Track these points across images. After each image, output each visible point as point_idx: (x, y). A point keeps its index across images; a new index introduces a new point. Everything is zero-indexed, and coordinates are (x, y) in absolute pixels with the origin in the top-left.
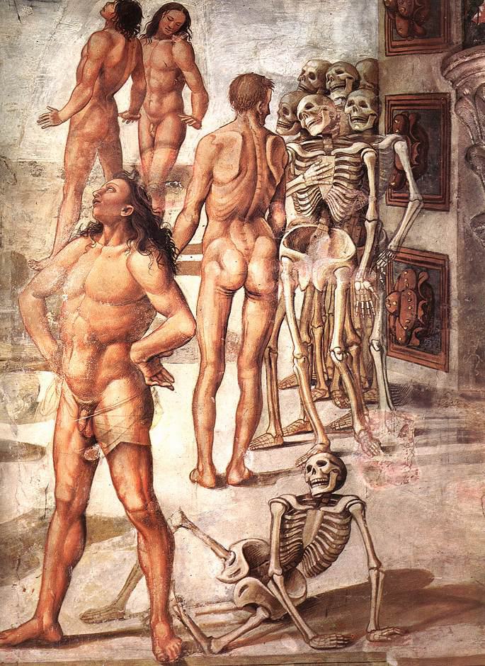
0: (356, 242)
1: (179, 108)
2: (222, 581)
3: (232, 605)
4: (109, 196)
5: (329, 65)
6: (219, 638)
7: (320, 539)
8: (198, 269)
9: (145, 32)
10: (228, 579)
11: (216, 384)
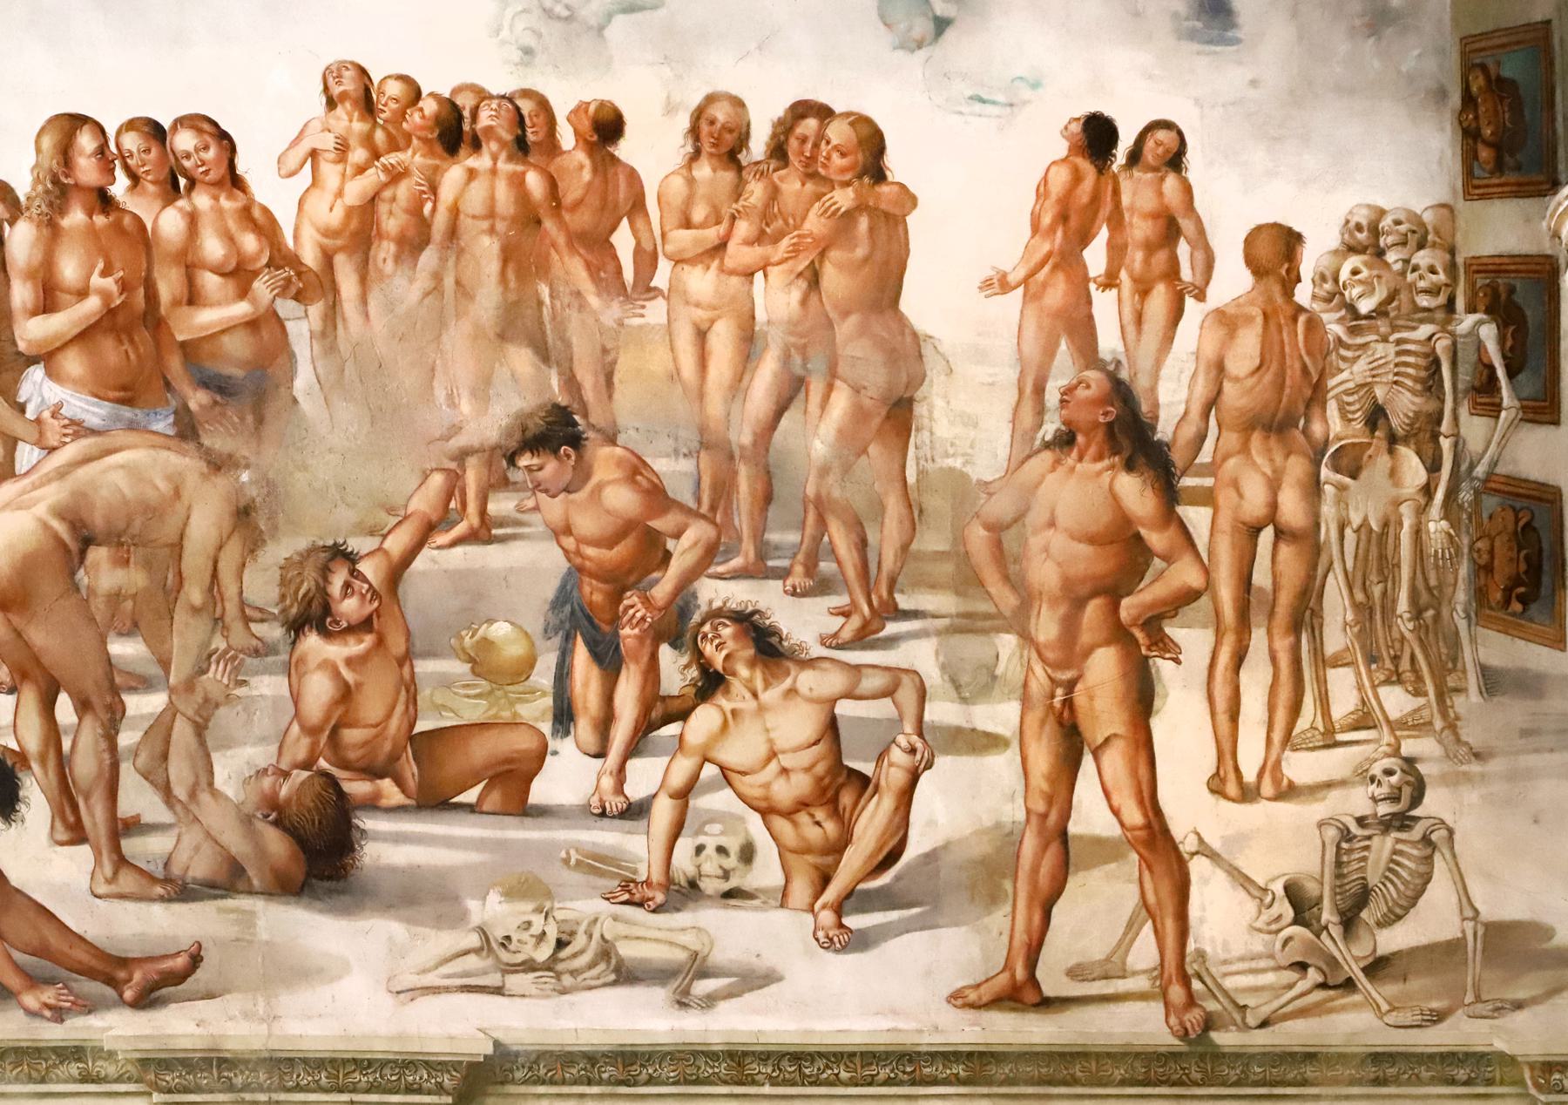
0: (1429, 462)
1: (1172, 272)
2: (1260, 930)
3: (1271, 963)
4: (1081, 393)
5: (1382, 213)
6: (1257, 1007)
7: (1391, 876)
8: (1206, 498)
9: (1124, 162)
10: (1265, 928)
11: (1239, 659)
